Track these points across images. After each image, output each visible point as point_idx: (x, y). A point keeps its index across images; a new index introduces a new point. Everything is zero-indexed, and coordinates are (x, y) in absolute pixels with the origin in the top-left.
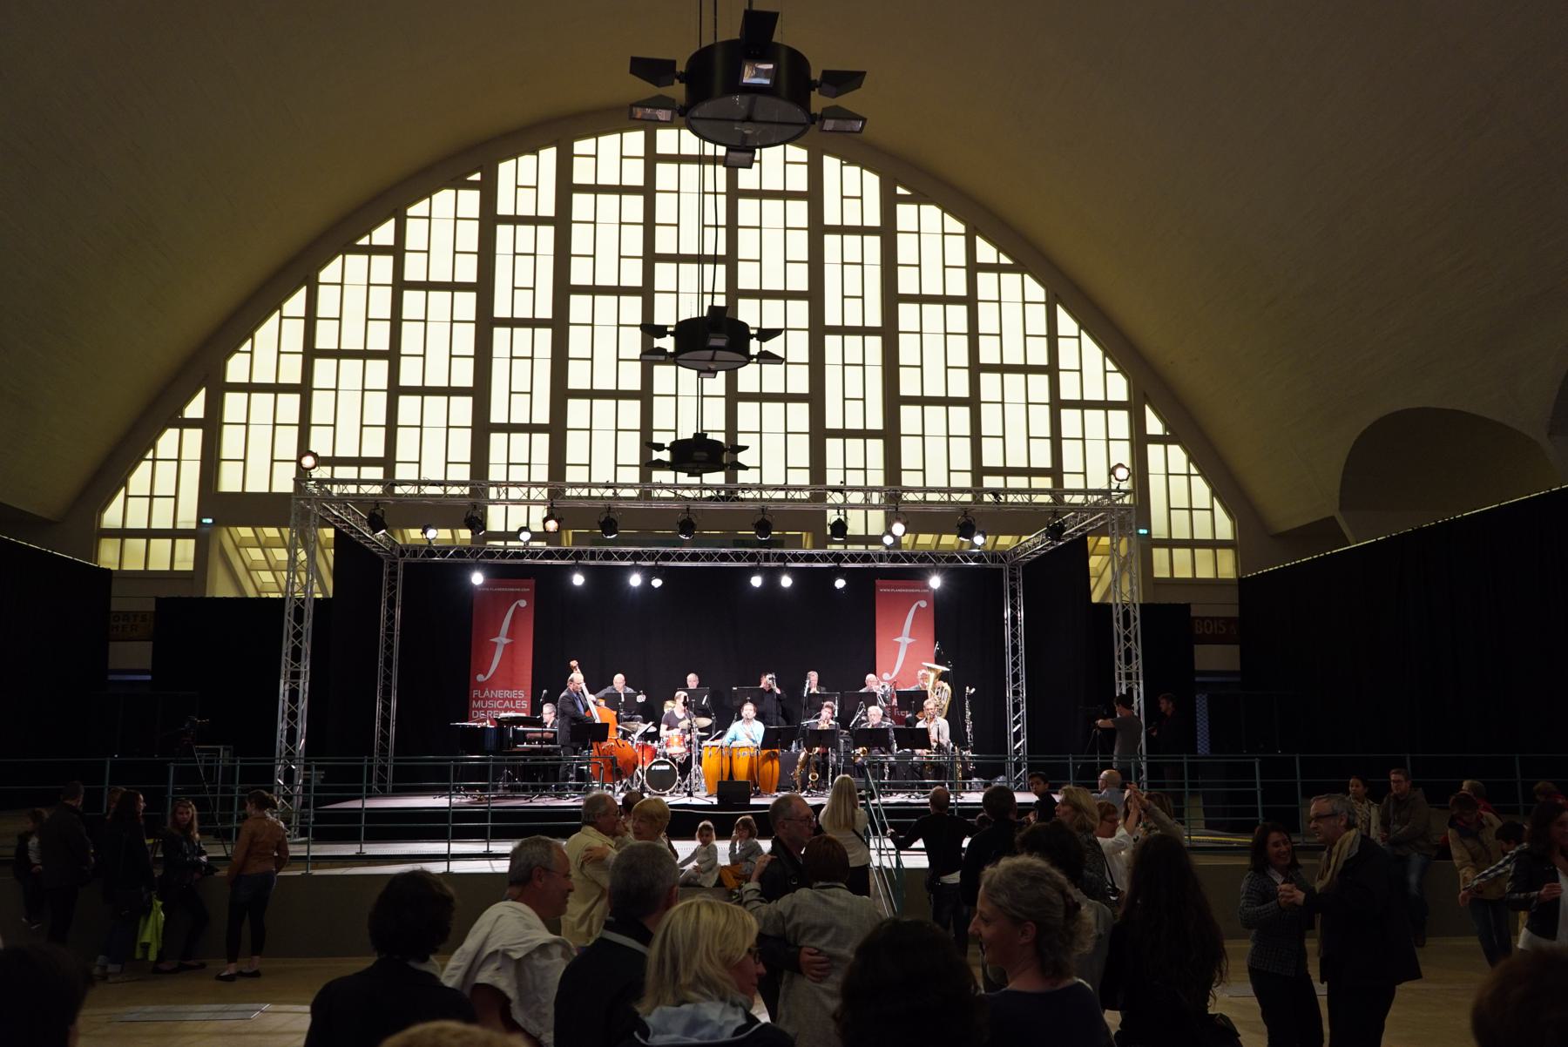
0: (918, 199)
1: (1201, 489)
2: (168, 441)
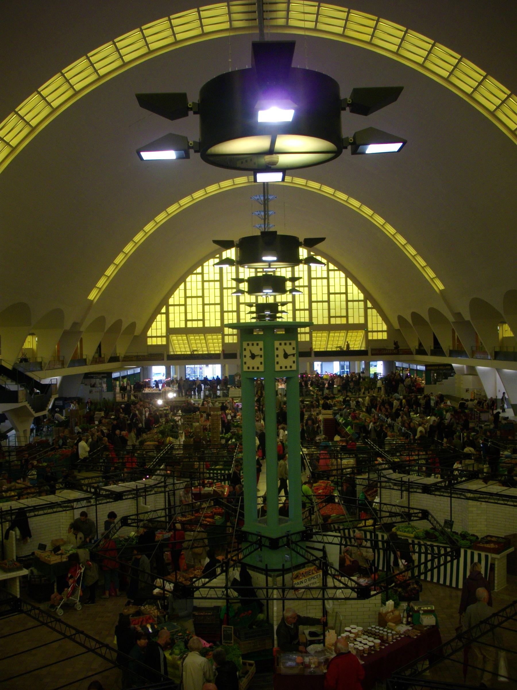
1: (380, 319)
2: (159, 317)
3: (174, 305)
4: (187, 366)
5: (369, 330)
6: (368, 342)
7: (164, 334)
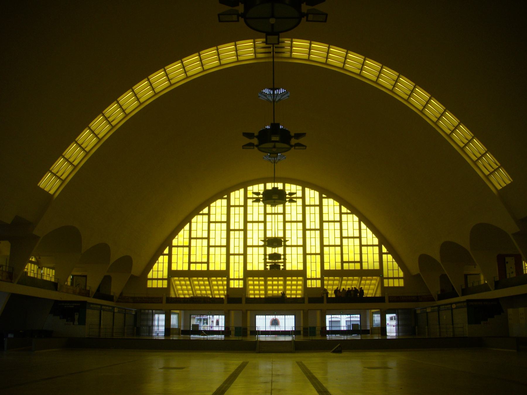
0: (328, 197)
1: (396, 264)
2: (161, 258)
3: (178, 246)
6: (384, 289)
7: (166, 277)
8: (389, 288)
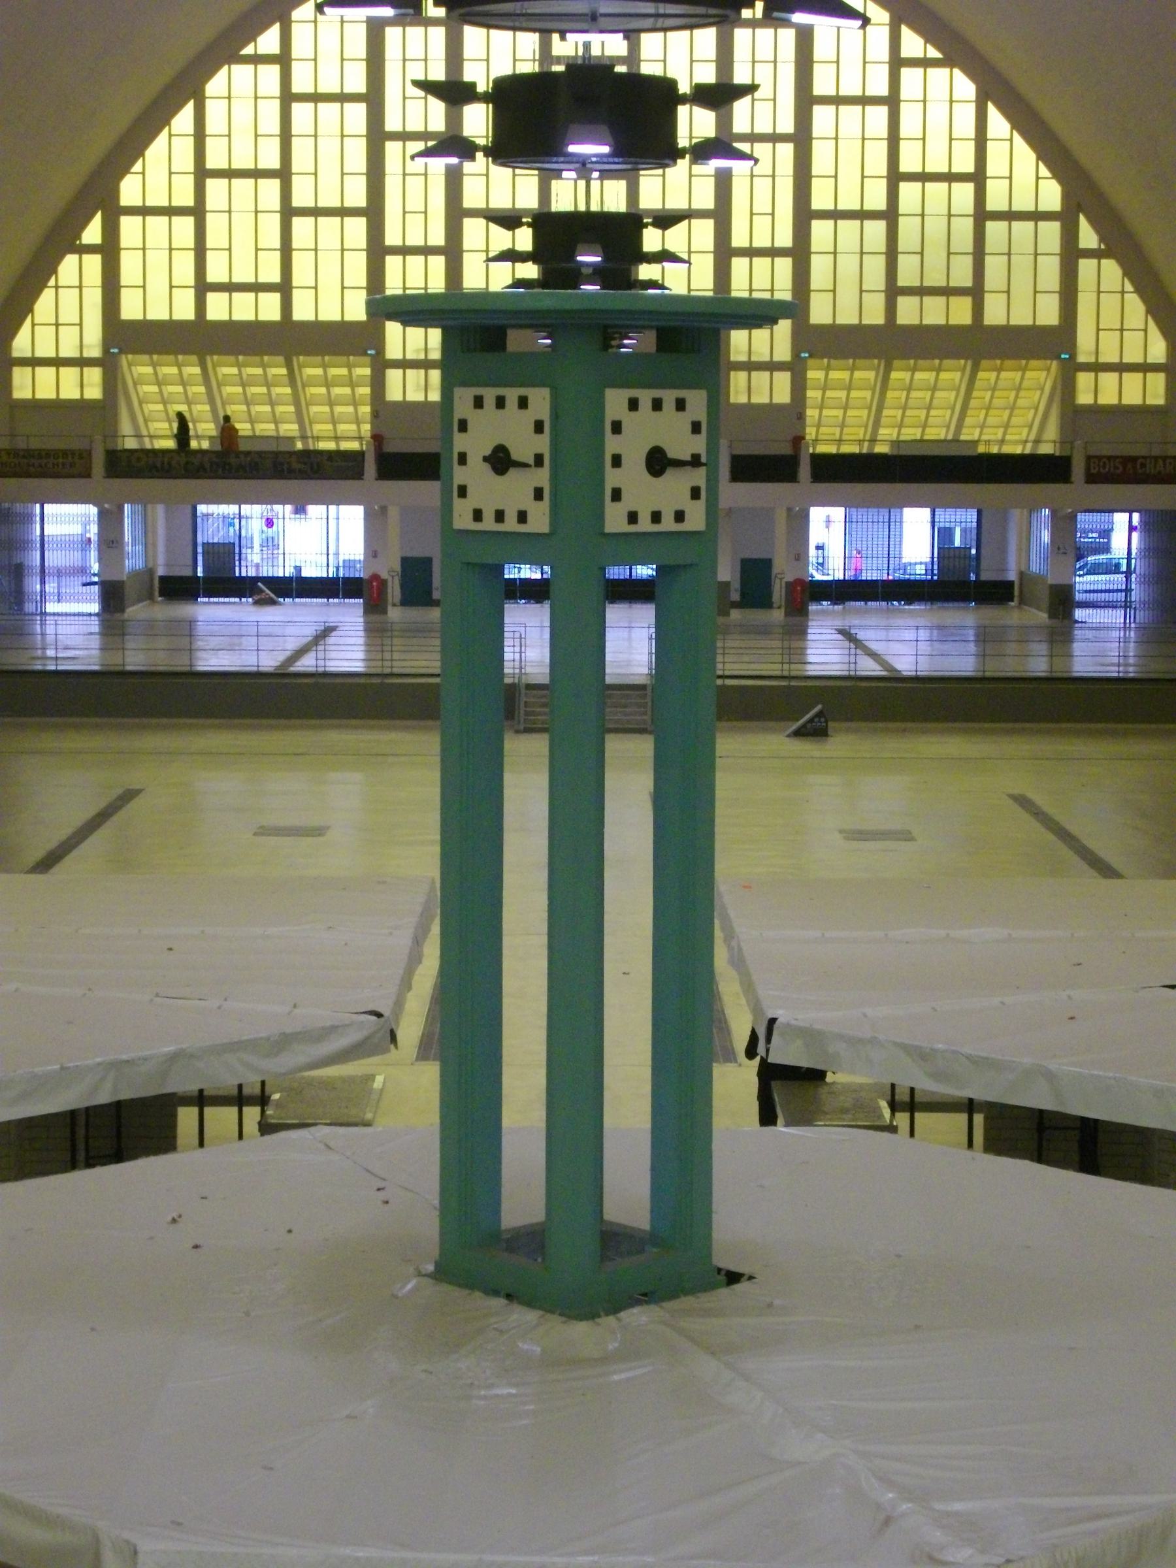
1: (1135, 306)
2: (69, 265)
3: (144, 211)
4: (202, 509)
5: (1082, 358)
8: (1096, 410)
